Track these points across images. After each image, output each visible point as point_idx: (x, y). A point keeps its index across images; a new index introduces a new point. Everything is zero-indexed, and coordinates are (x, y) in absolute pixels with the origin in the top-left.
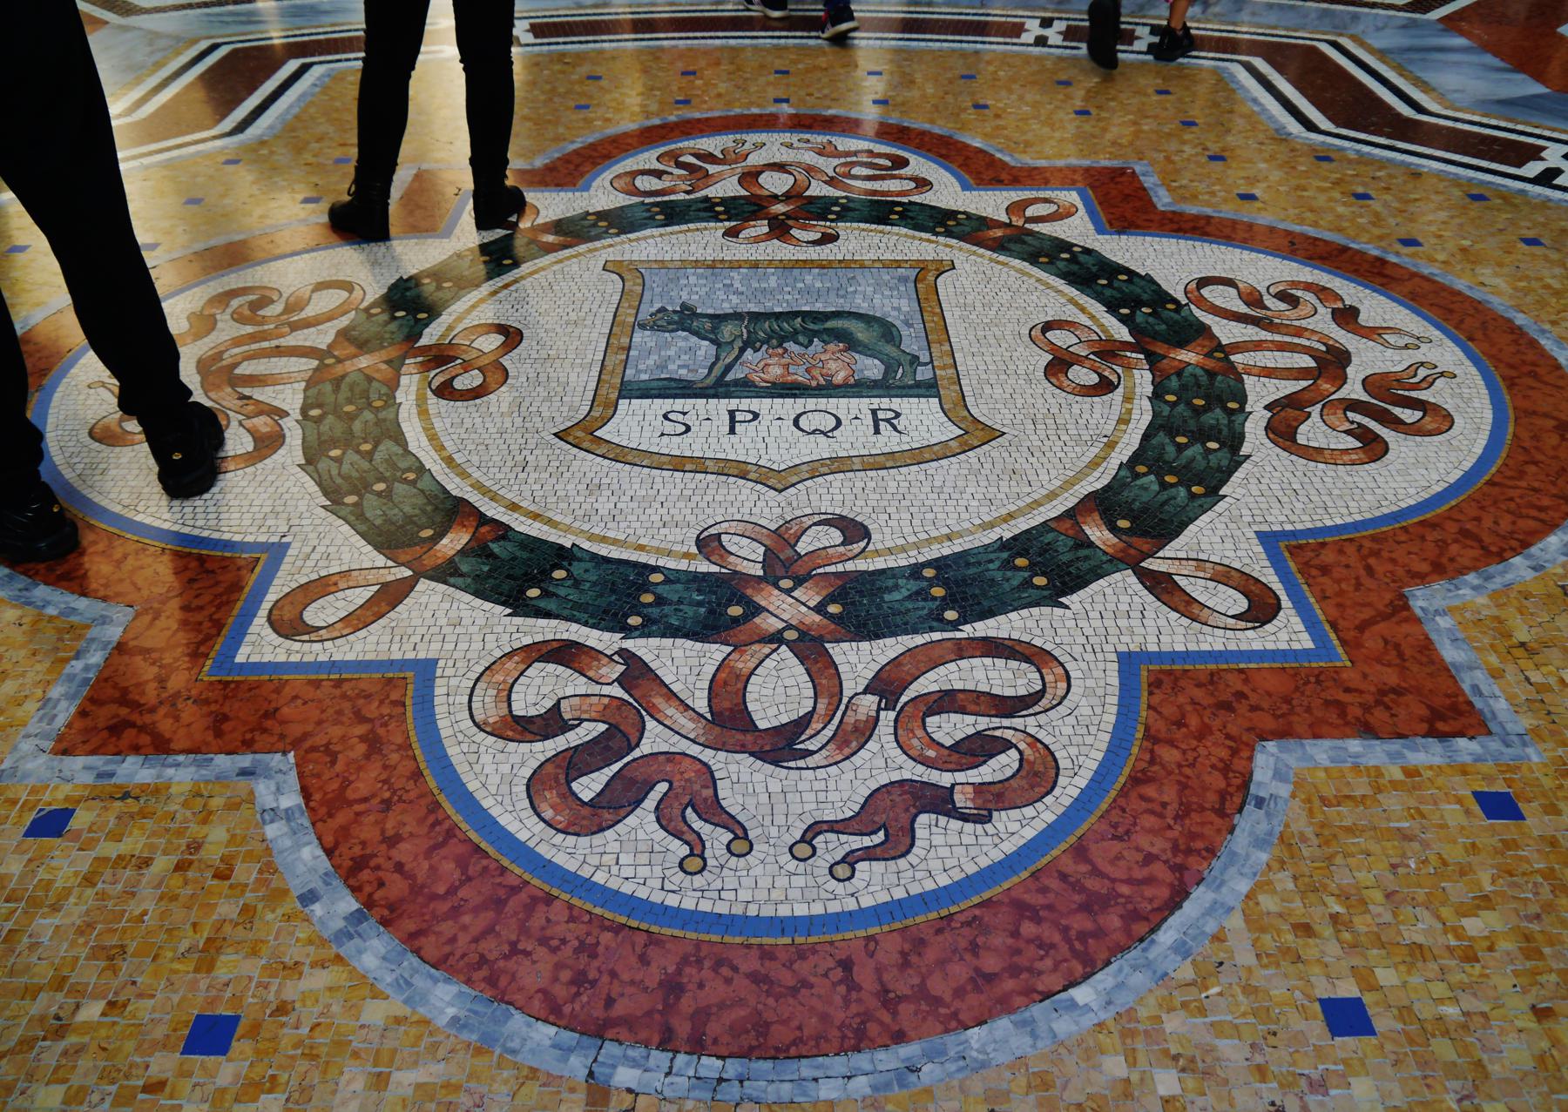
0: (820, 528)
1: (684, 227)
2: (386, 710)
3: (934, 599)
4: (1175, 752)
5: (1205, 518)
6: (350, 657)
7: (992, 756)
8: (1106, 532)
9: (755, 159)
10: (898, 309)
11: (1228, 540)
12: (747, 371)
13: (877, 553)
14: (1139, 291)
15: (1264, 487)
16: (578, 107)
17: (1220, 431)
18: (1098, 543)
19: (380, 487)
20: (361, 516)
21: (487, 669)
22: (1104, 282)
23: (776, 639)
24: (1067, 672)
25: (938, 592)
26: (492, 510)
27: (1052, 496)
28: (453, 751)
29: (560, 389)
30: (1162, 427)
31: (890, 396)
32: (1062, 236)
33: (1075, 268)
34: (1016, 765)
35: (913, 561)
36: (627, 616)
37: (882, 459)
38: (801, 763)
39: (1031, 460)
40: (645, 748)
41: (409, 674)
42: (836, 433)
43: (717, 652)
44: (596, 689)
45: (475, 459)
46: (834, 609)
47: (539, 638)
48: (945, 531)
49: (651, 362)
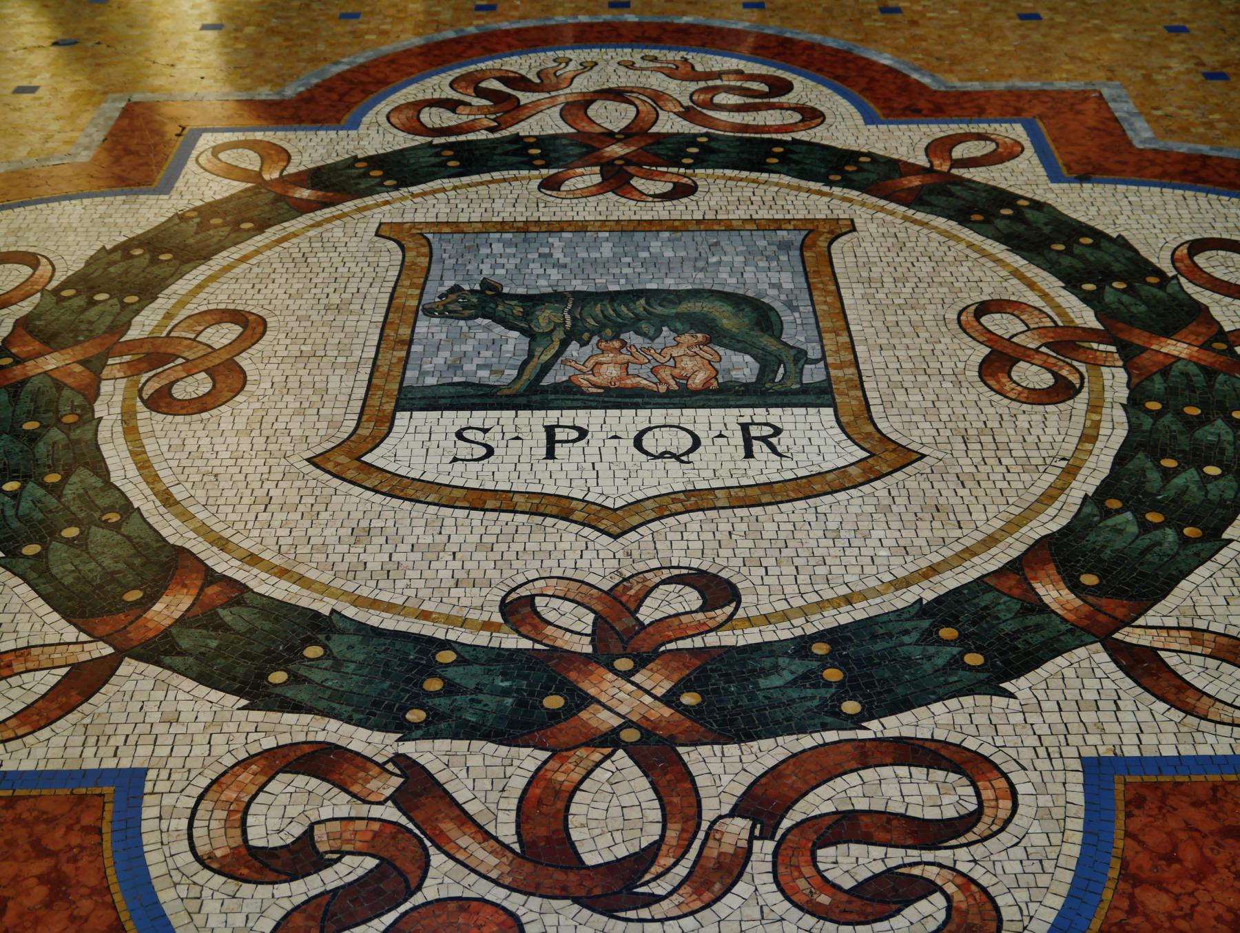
0: (670, 587)
1: (486, 177)
2: (75, 840)
3: (828, 684)
4: (1164, 897)
5: (1203, 571)
6: (27, 766)
7: (908, 903)
8: (1065, 592)
9: (583, 84)
10: (778, 286)
12: (571, 372)
13: (750, 621)
14: (1108, 258)
16: (345, 16)
17: (1222, 452)
18: (1054, 606)
19: (71, 532)
21: (214, 782)
22: (1061, 247)
23: (610, 740)
24: (1012, 786)
25: (833, 675)
26: (222, 564)
27: (990, 541)
28: (166, 896)
29: (316, 398)
30: (1141, 445)
31: (767, 406)
32: (1003, 186)
33: (1021, 228)
34: (941, 916)
35: (798, 632)
36: (405, 709)
37: (756, 491)
38: (644, 913)
39: (961, 492)
40: (430, 891)
41: (108, 790)
42: (692, 456)
43: (529, 759)
44: (362, 810)
45: (200, 494)
46: (689, 699)
47: (285, 740)
48: (844, 590)
49: (439, 361)
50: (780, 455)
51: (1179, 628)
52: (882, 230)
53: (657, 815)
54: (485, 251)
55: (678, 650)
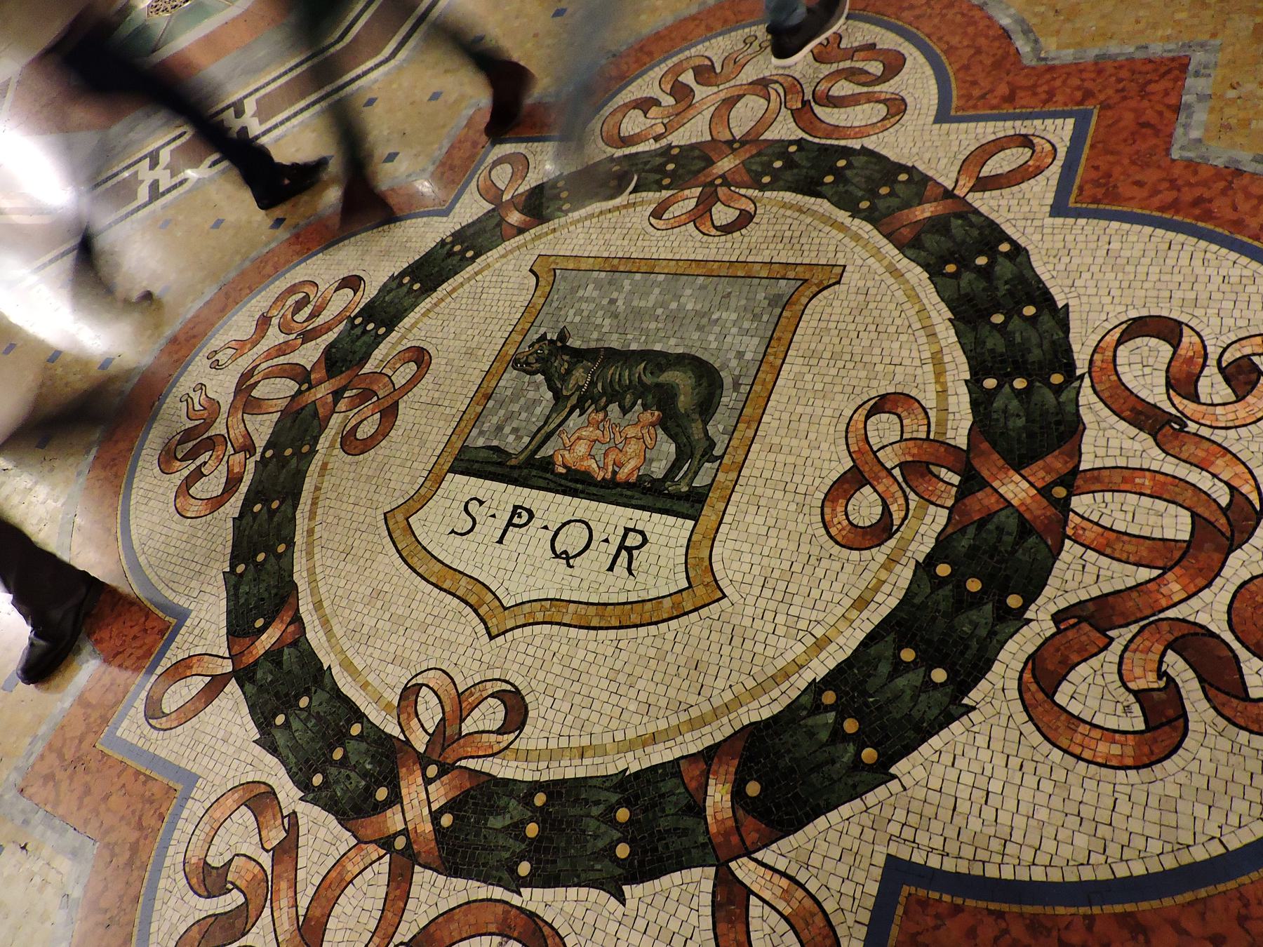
10: (740, 355)
11: (848, 859)
14: (1035, 339)
15: (952, 774)
18: (709, 811)
20: (236, 587)
48: (585, 741)
50: (630, 572)
51: (783, 874)
52: (861, 283)
53: (372, 925)
54: (580, 293)
55: (465, 768)
